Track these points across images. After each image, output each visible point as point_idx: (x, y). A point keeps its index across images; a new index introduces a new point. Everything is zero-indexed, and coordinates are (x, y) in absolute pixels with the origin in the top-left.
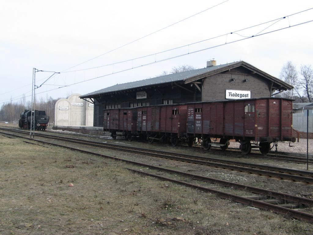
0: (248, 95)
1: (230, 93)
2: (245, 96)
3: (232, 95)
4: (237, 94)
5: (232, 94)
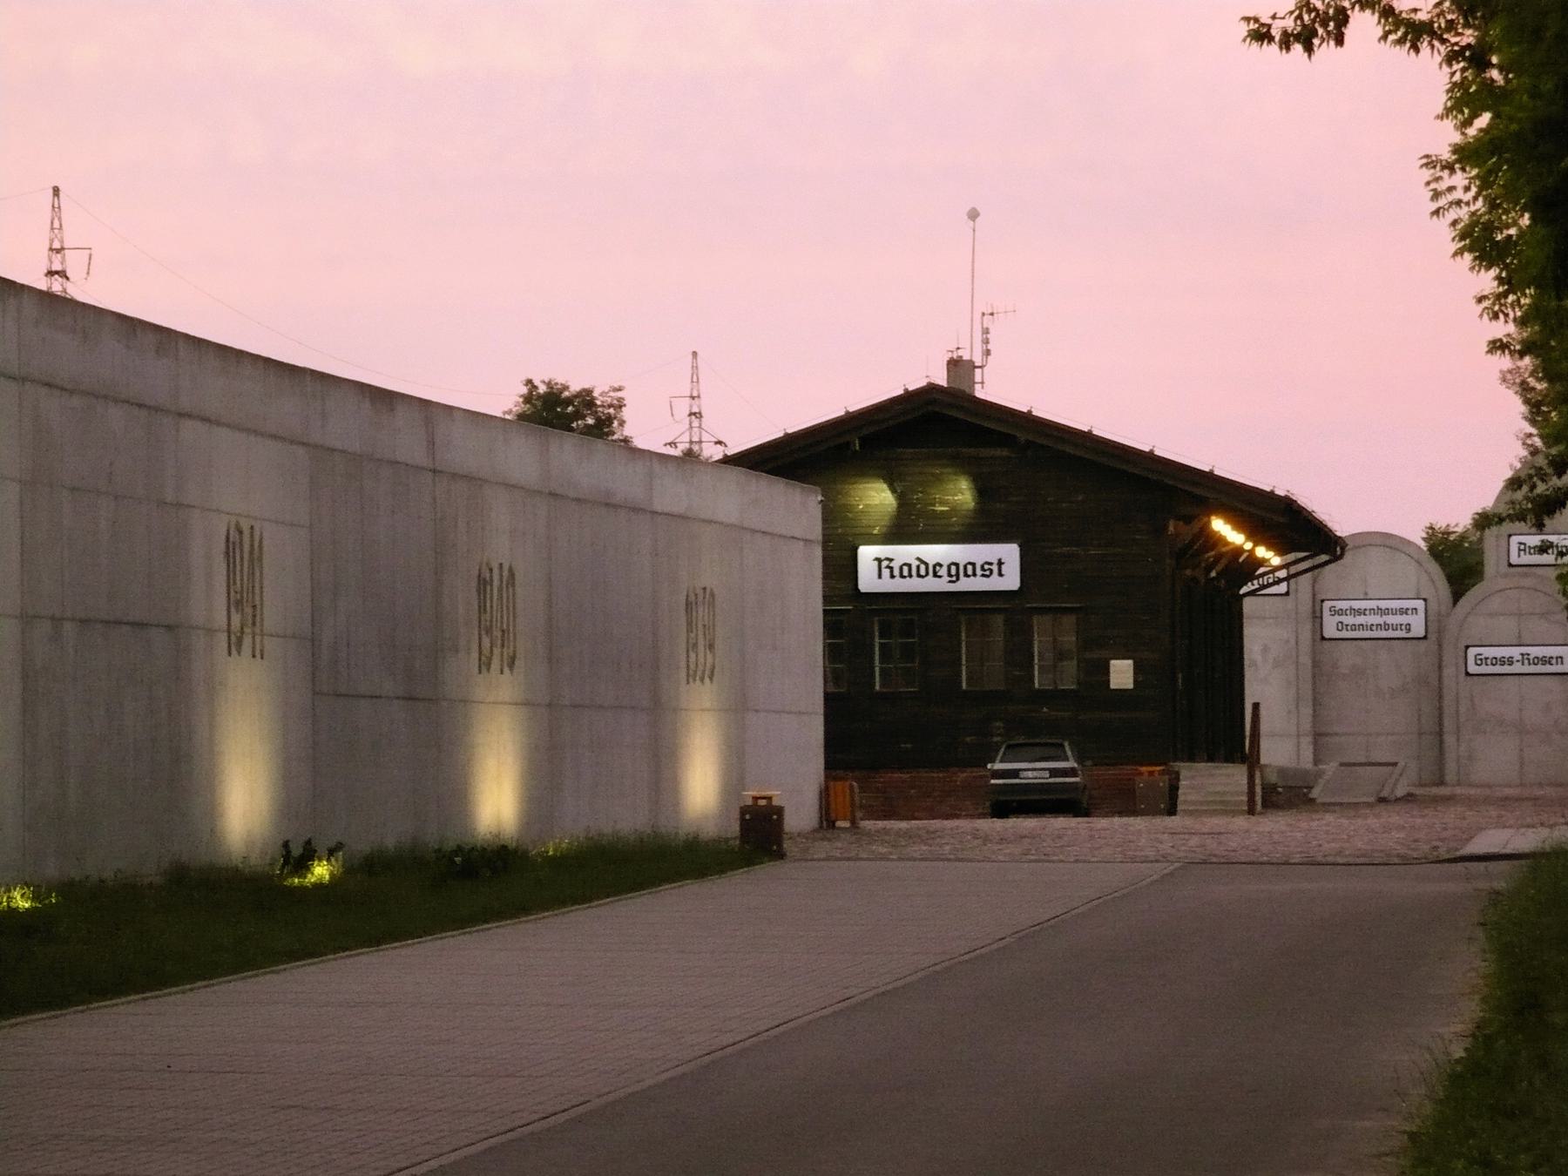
0: (1000, 563)
1: (885, 563)
2: (979, 572)
3: (896, 572)
4: (926, 564)
5: (896, 565)
